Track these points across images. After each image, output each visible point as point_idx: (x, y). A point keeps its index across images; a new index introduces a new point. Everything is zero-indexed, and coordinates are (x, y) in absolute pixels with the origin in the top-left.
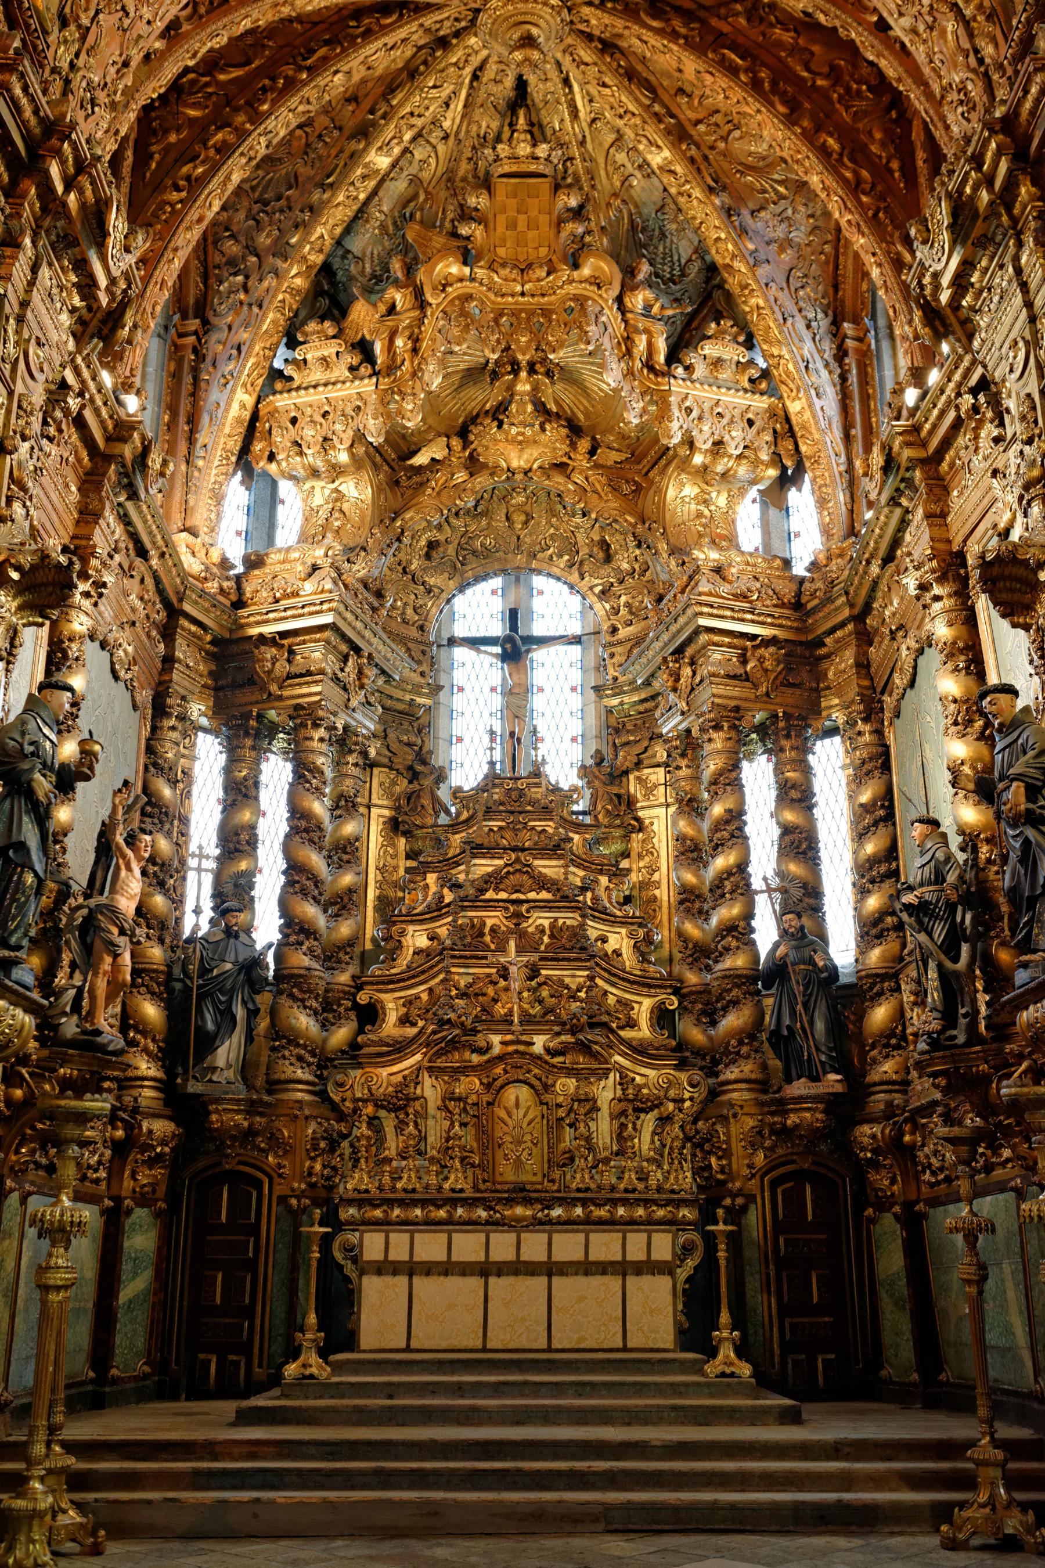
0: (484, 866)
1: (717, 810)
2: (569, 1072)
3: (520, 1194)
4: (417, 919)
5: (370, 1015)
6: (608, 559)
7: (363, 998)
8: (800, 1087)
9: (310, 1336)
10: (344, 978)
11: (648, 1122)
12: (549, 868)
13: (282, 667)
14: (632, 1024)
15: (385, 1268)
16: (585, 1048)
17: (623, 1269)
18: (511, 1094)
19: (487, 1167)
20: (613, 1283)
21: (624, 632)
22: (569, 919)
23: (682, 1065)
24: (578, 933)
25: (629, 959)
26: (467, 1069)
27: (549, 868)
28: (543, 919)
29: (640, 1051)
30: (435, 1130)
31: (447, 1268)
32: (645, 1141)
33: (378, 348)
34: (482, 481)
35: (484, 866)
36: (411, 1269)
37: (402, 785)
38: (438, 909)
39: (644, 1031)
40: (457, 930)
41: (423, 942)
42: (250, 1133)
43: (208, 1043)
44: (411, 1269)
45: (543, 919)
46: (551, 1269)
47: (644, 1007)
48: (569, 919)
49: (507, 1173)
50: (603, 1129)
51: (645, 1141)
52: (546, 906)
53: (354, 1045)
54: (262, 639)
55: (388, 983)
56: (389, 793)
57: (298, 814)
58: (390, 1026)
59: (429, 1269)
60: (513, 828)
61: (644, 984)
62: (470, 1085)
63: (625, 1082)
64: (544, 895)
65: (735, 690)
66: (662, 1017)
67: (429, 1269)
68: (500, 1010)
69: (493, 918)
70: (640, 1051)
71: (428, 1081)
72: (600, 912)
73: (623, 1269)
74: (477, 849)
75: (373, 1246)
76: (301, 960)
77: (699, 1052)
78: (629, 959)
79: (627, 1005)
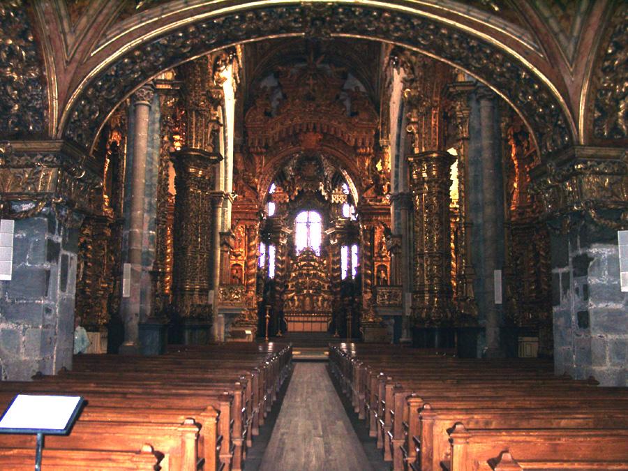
0: (303, 263)
3: (308, 312)
5: (288, 286)
8: (346, 299)
10: (283, 281)
11: (326, 303)
12: (312, 263)
15: (291, 321)
17: (321, 322)
18: (308, 298)
20: (320, 324)
22: (315, 272)
23: (332, 294)
25: (325, 278)
27: (312, 263)
28: (312, 272)
30: (296, 303)
31: (299, 321)
32: (325, 305)
35: (303, 263)
36: (294, 321)
38: (295, 271)
41: (294, 275)
44: (294, 321)
45: (312, 272)
46: (312, 322)
47: (326, 285)
48: (315, 272)
50: (320, 303)
51: (325, 305)
52: (313, 270)
55: (289, 282)
57: (277, 260)
59: (296, 322)
61: (327, 282)
62: (301, 298)
63: (323, 297)
69: (304, 272)
70: (325, 292)
72: (320, 271)
73: (321, 322)
75: (289, 319)
76: (278, 280)
78: (325, 278)
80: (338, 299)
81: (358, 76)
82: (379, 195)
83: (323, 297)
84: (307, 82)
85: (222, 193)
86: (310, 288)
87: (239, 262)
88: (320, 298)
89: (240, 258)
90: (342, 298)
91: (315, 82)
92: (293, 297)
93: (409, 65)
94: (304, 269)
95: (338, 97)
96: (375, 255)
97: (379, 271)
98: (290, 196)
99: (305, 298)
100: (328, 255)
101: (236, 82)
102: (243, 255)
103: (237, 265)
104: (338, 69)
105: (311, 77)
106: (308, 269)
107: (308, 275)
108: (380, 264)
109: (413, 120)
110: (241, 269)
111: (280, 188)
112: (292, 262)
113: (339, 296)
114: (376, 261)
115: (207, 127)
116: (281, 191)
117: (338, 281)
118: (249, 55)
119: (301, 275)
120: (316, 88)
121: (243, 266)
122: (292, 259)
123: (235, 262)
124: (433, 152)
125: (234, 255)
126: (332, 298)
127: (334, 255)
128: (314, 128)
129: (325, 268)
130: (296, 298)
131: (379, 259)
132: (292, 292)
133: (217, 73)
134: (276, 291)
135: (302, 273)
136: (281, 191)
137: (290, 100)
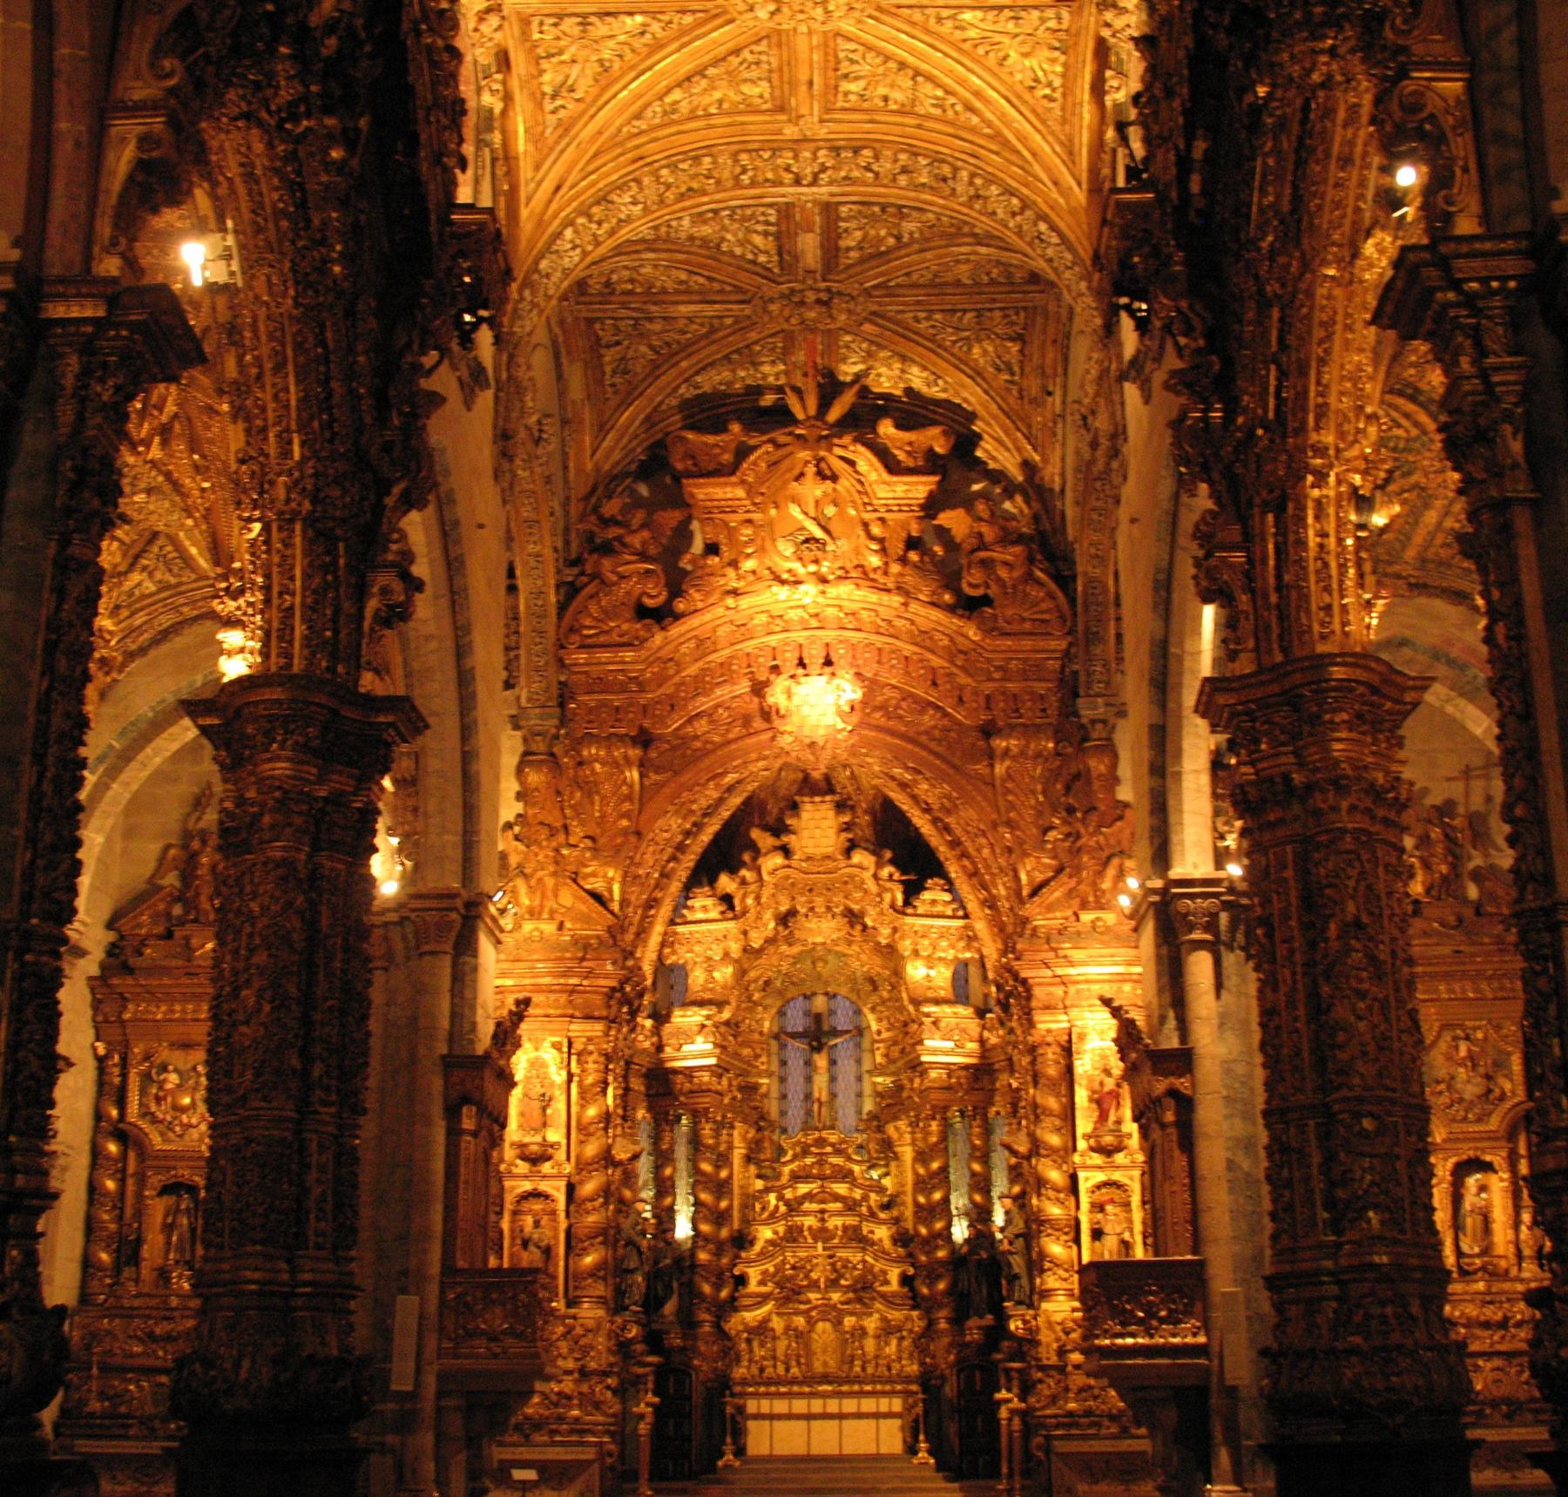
0: (803, 1189)
1: (935, 1165)
2: (852, 1314)
3: (826, 1379)
4: (765, 1223)
5: (742, 1280)
6: (875, 989)
7: (736, 1272)
9: (728, 1449)
12: (841, 1188)
13: (687, 1086)
14: (887, 1282)
15: (759, 1416)
16: (860, 1300)
17: (877, 1416)
18: (820, 1325)
19: (809, 1365)
20: (872, 1422)
21: (885, 1035)
22: (851, 1221)
23: (914, 1308)
24: (857, 1229)
26: (797, 1313)
29: (887, 1299)
33: (737, 902)
34: (796, 949)
35: (803, 1189)
37: (752, 1133)
38: (773, 1217)
39: (894, 1285)
40: (790, 1229)
42: (683, 1349)
43: (660, 1303)
46: (841, 1416)
47: (894, 1274)
49: (818, 1367)
50: (870, 1345)
51: (891, 1349)
52: (839, 1213)
53: (733, 1299)
54: (675, 1071)
55: (749, 1262)
56: (744, 1138)
58: (753, 1286)
59: (780, 1417)
60: (821, 1163)
62: (800, 1321)
64: (838, 1206)
65: (945, 1095)
66: (905, 1280)
67: (780, 1417)
68: (814, 1275)
70: (887, 1299)
71: (775, 1318)
73: (877, 1416)
74: (796, 1178)
77: (924, 1298)
78: (887, 1244)
79: (884, 1272)
80: (943, 1325)
82: (1084, 906)
83: (884, 1319)
85: (452, 896)
86: (833, 1284)
87: (544, 1186)
88: (871, 1324)
89: (547, 1168)
90: (958, 1321)
92: (766, 1320)
94: (806, 1213)
96: (1082, 1145)
97: (1099, 1207)
98: (745, 933)
99: (811, 1323)
100: (896, 1157)
102: (561, 1155)
103: (536, 1195)
106: (823, 1211)
107: (822, 1234)
108: (1100, 1177)
110: (554, 1213)
111: (709, 902)
112: (759, 1184)
113: (943, 1313)
114: (1086, 1167)
116: (714, 914)
117: (941, 1254)
119: (793, 1235)
121: (561, 1198)
122: (759, 1176)
123: (527, 1186)
125: (524, 1158)
126: (916, 1320)
127: (921, 1157)
128: (828, 662)
129: (886, 1207)
130: (777, 1324)
131: (1097, 1159)
132: (764, 1299)
134: (701, 1295)
135: (800, 1229)
136: (714, 914)
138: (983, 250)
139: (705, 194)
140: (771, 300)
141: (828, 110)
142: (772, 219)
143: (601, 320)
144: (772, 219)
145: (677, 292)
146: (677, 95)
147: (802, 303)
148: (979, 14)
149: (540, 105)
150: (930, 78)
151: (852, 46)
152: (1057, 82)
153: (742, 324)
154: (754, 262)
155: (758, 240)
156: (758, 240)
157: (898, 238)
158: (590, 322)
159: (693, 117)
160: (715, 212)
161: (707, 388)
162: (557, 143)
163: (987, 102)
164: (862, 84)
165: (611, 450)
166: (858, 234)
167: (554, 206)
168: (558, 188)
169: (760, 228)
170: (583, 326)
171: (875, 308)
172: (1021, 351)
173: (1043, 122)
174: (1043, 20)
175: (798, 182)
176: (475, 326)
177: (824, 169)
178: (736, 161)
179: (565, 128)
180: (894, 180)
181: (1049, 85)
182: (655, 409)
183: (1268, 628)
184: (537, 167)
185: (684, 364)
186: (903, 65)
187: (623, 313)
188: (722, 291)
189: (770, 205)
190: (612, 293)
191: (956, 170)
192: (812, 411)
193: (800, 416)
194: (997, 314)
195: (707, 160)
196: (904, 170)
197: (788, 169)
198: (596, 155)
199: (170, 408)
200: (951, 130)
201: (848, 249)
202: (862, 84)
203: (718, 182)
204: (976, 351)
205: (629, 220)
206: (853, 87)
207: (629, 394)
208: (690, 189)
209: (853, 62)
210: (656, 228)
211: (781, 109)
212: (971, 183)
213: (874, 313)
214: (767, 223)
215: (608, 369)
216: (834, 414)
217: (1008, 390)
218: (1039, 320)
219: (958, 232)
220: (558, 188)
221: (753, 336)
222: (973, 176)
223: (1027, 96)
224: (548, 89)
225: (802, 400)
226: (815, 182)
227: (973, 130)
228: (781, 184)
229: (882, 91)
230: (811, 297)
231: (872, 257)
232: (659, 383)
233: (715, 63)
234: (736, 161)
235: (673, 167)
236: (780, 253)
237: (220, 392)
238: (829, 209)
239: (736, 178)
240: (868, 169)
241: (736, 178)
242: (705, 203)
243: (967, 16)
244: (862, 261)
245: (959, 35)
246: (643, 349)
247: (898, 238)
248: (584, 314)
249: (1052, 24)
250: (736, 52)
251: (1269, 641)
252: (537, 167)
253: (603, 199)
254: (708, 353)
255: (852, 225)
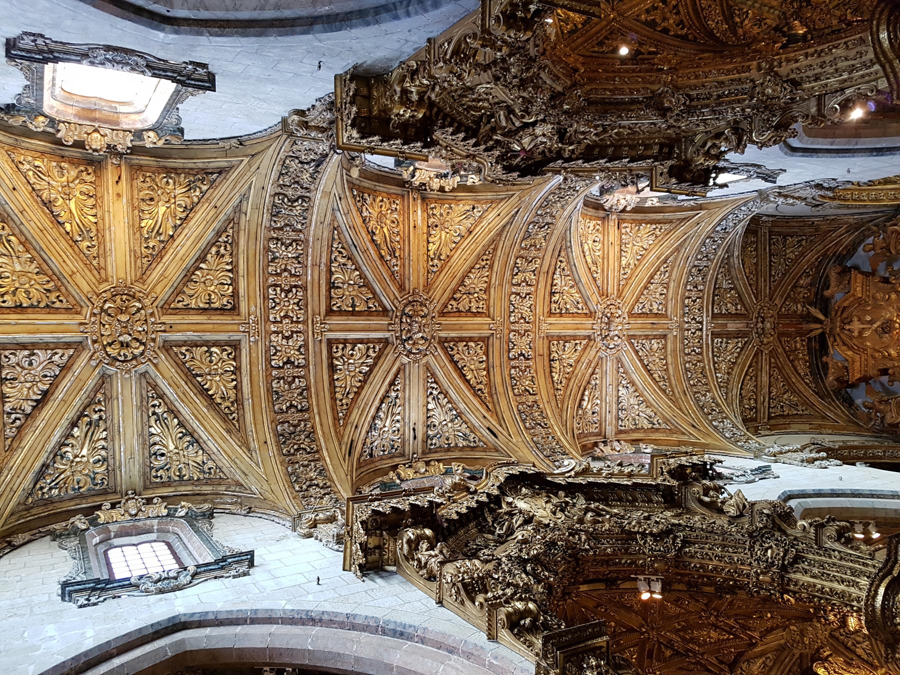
81: (852, 249)
84: (856, 334)
91: (855, 319)
93: (709, 144)
95: (886, 281)
101: (823, 459)
104: (833, 283)
105: (848, 327)
109: (813, 110)
115: (827, 552)
118: (807, 427)
120: (868, 318)
124: (877, 42)
133: (725, 508)
137: (889, 364)
138: (736, 253)
139: (704, 367)
140: (762, 342)
141: (667, 317)
142: (720, 340)
143: (769, 413)
144: (720, 340)
145: (756, 381)
146: (655, 376)
147: (763, 329)
148: (623, 258)
149: (657, 429)
150: (652, 277)
151: (636, 307)
152: (654, 226)
153: (773, 354)
154: (742, 349)
155: (730, 346)
156: (730, 346)
157: (732, 289)
158: (770, 418)
159: (667, 370)
160: (715, 363)
161: (808, 371)
162: (673, 425)
163: (662, 254)
164: (654, 303)
165: (835, 414)
166: (729, 305)
167: (702, 429)
168: (693, 426)
169: (724, 345)
170: (772, 422)
171: (767, 299)
172: (792, 237)
173: (671, 230)
174: (627, 233)
175: (701, 330)
176: (714, 470)
177: (694, 319)
178: (689, 354)
179: (667, 420)
180: (700, 291)
181: (654, 229)
182: (816, 393)
183: (863, 76)
184: (684, 434)
185: (794, 380)
186: (646, 288)
187: (766, 404)
188: (756, 363)
189: (713, 341)
190: (756, 408)
191: (695, 266)
192: (819, 326)
193: (821, 331)
194: (773, 247)
195: (687, 365)
196: (696, 287)
197: (694, 333)
198: (681, 410)
199: (731, 622)
200: (676, 268)
201: (737, 310)
202: (654, 303)
203: (699, 361)
204: (792, 256)
205: (713, 398)
206: (655, 306)
207: (807, 404)
208: (701, 373)
209: (644, 307)
210: (720, 387)
211: (665, 337)
212: (701, 260)
213: (770, 300)
214: (721, 342)
215: (795, 412)
216: (822, 317)
217: (811, 241)
218: (776, 229)
219: (726, 263)
220: (693, 426)
221: (780, 350)
222: (698, 260)
223: (660, 238)
224: (650, 426)
225: (811, 331)
226: (701, 323)
227: (676, 259)
228: (701, 336)
229: (658, 296)
230: (760, 325)
231: (741, 300)
232: (803, 390)
233: (641, 361)
234: (689, 354)
235: (689, 379)
236: (737, 338)
237: (721, 597)
238: (714, 316)
239: (698, 354)
240: (694, 301)
241: (698, 354)
242: (709, 367)
243: (624, 263)
244: (743, 305)
245: (632, 266)
246: (785, 396)
247: (732, 289)
248: (766, 420)
249: (628, 230)
250: (637, 352)
251: (869, 75)
252: (684, 434)
253: (702, 408)
254: (789, 370)
255: (723, 308)
